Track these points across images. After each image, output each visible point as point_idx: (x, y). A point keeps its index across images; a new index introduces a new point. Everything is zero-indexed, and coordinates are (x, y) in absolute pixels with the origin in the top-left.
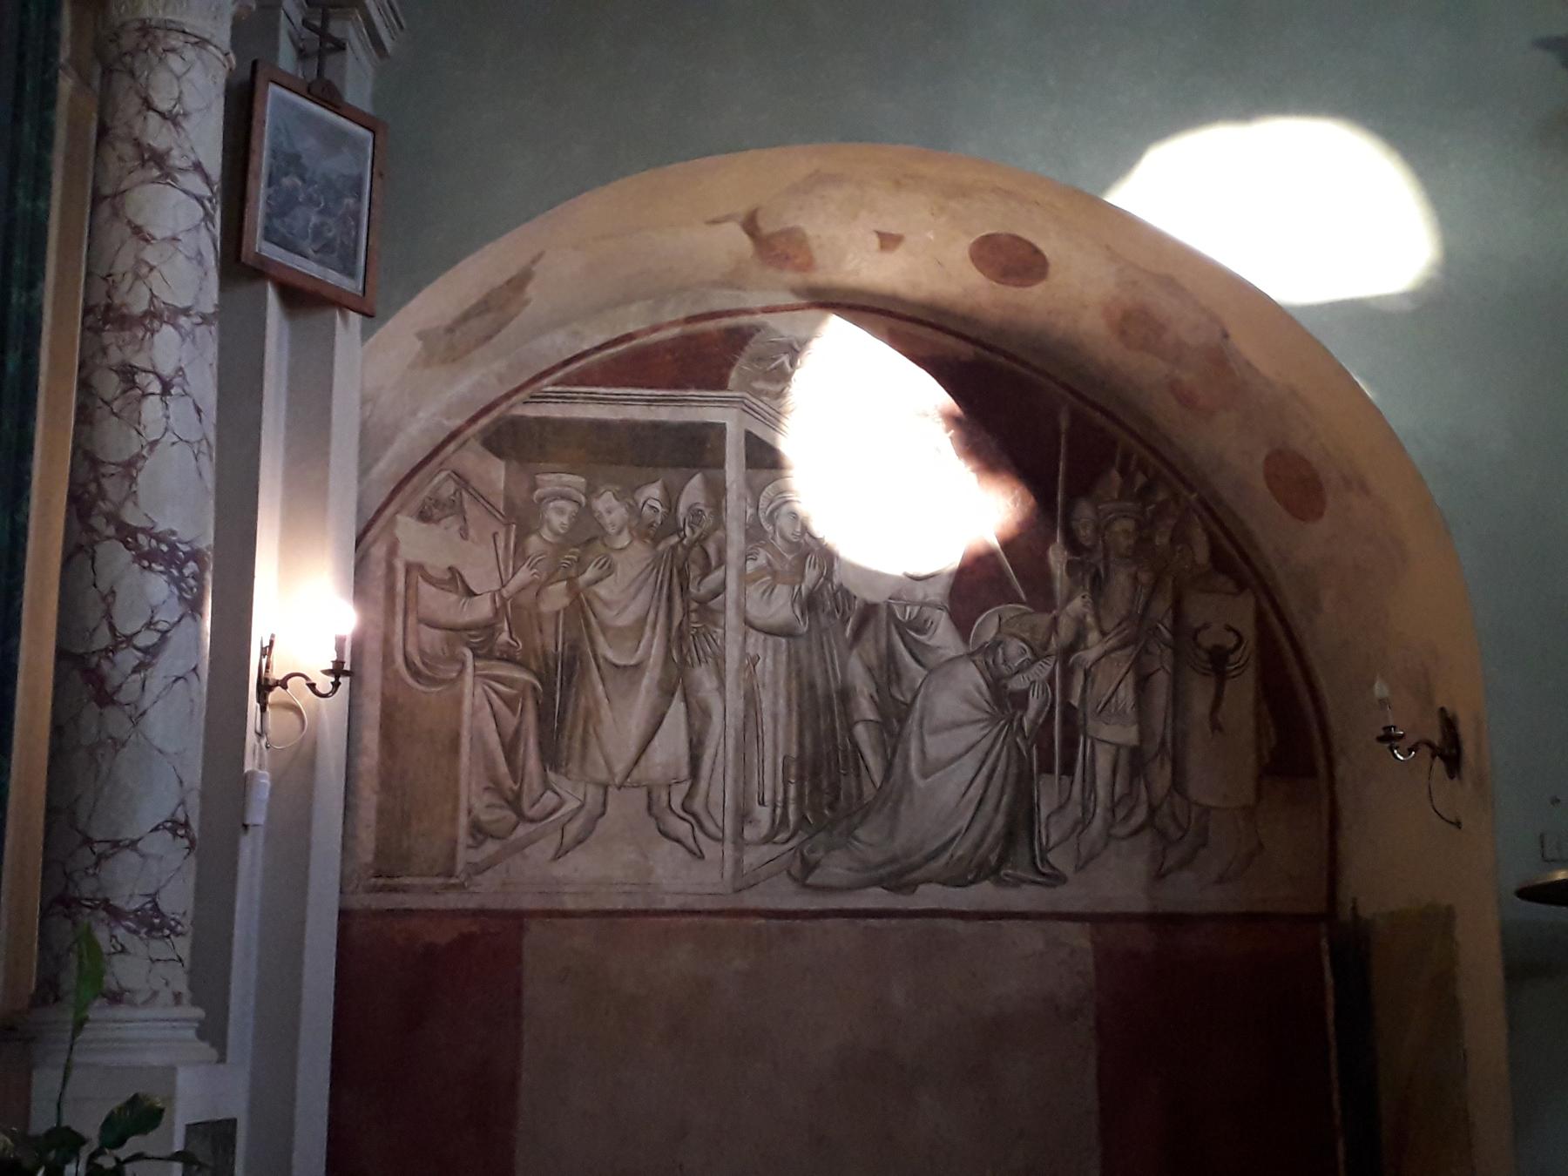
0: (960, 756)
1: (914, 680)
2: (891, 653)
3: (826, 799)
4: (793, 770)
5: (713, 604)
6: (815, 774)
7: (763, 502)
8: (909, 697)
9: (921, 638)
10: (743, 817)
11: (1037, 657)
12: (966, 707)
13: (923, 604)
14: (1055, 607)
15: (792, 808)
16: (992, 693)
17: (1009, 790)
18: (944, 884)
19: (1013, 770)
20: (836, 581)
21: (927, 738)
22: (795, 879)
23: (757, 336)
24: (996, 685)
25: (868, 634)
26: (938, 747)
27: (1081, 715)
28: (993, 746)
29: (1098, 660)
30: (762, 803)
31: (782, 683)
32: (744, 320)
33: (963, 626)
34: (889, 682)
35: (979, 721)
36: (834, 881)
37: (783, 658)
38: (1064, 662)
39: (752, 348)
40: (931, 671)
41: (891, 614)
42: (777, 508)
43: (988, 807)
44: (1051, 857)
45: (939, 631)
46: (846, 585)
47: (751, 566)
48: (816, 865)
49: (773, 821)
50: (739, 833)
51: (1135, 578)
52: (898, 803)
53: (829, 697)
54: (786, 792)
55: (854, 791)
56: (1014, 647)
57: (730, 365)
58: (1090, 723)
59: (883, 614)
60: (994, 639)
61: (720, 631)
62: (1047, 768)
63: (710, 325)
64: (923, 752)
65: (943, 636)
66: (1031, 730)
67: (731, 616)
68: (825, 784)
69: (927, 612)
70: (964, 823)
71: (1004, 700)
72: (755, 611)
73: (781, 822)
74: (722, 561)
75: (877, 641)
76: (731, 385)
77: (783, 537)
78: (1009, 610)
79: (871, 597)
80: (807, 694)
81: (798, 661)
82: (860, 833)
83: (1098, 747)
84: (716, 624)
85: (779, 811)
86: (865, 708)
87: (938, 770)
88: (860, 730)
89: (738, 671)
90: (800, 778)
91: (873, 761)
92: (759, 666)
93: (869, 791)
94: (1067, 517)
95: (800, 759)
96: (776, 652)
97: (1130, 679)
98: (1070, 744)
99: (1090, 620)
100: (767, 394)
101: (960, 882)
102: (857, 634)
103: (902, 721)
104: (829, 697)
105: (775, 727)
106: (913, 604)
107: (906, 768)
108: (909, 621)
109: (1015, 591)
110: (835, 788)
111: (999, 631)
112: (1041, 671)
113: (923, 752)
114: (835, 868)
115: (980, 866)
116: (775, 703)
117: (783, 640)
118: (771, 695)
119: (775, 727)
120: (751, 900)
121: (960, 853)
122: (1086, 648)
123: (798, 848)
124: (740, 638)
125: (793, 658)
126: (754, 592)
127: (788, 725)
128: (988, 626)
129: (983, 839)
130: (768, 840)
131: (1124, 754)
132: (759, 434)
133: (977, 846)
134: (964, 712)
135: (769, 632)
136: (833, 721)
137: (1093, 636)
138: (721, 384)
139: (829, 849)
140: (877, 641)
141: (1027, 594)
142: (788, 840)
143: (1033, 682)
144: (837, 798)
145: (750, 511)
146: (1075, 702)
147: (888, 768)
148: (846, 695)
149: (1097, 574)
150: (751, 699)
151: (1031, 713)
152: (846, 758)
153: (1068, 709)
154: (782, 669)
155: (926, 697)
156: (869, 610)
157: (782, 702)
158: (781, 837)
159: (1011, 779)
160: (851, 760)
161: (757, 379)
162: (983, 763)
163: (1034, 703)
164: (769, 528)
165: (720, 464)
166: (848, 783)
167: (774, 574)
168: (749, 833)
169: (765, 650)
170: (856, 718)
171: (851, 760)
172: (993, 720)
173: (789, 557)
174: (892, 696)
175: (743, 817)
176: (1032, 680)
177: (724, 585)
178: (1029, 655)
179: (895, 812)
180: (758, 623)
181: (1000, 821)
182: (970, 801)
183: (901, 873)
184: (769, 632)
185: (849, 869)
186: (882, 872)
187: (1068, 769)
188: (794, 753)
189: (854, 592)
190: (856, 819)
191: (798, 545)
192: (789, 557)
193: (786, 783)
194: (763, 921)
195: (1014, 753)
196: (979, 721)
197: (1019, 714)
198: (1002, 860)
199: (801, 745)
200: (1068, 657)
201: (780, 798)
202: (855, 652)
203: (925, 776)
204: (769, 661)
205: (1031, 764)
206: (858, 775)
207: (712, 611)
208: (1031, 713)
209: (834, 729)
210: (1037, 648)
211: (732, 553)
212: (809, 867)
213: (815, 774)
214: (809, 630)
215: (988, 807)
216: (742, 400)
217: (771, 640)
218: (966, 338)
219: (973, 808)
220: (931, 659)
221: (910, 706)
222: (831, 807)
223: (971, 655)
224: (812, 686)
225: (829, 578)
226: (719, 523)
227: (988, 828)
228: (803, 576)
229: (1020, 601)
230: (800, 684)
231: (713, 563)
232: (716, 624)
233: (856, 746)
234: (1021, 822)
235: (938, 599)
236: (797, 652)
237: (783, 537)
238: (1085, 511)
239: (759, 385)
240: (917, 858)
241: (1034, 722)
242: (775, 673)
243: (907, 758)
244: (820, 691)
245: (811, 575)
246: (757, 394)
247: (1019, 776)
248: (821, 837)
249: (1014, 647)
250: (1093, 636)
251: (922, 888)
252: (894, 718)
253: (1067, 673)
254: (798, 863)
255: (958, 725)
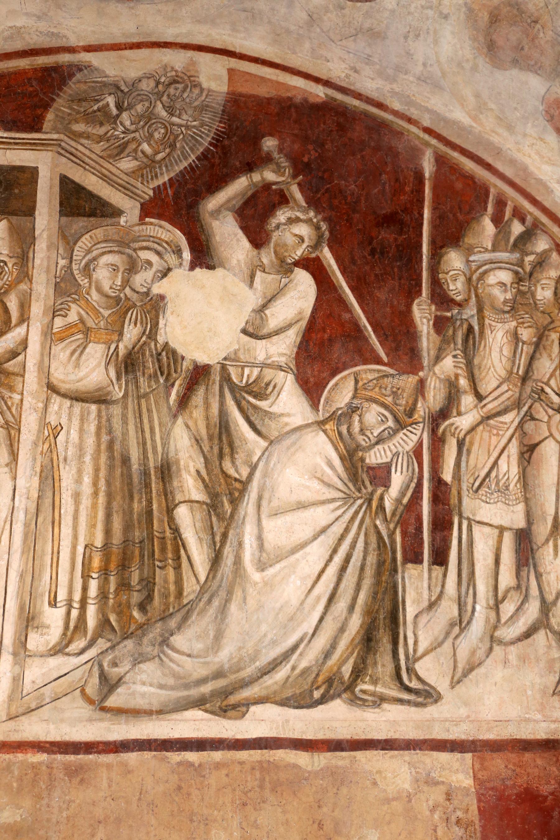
0: (303, 545)
1: (250, 455)
2: (223, 413)
3: (136, 598)
4: (96, 562)
5: (10, 366)
6: (124, 566)
7: (78, 253)
8: (245, 472)
9: (263, 404)
10: (29, 620)
11: (401, 425)
12: (316, 485)
13: (264, 365)
14: (422, 368)
15: (92, 611)
16: (346, 469)
17: (367, 583)
18: (284, 703)
19: (372, 559)
20: (161, 339)
21: (264, 522)
22: (91, 702)
23: (78, 76)
24: (352, 459)
25: (198, 398)
26: (279, 531)
27: (454, 492)
28: (347, 530)
29: (473, 429)
30: (53, 603)
31: (88, 459)
32: (65, 58)
33: (312, 390)
34: (221, 456)
35: (333, 500)
36: (141, 703)
37: (92, 428)
38: (434, 431)
39: (73, 87)
40: (271, 443)
41: (226, 378)
42: (95, 259)
43: (341, 605)
44: (420, 667)
45: (283, 395)
46: (172, 344)
47: (59, 322)
48: (119, 681)
49: (67, 627)
50: (22, 643)
51: (516, 337)
52: (228, 601)
53: (146, 473)
54: (85, 589)
55: (172, 587)
56: (373, 415)
57: (46, 106)
58: (466, 501)
59: (216, 377)
60: (349, 405)
61: (17, 397)
62: (417, 559)
63: (23, 63)
64: (260, 538)
65: (288, 402)
66: (394, 514)
67: (32, 380)
68: (135, 578)
69: (269, 374)
70: (309, 626)
71: (361, 474)
72: (63, 373)
73: (76, 628)
74: (24, 319)
75: (207, 405)
76: (47, 126)
77: (99, 290)
78: (368, 372)
79: (203, 359)
80: (118, 471)
81: (110, 432)
82: (178, 640)
83: (476, 529)
84: (11, 389)
85: (75, 613)
86: (189, 486)
87: (279, 559)
88: (183, 514)
89: (35, 444)
90: (105, 571)
91: (198, 552)
92: (61, 438)
93: (190, 587)
94: (434, 270)
95: (106, 546)
96: (82, 420)
97: (514, 449)
98: (442, 525)
99: (463, 382)
100: (88, 138)
101: (302, 701)
102: (184, 401)
103: (235, 502)
104: (146, 473)
105: (77, 511)
106: (253, 365)
107: (238, 561)
108: (247, 385)
109: (373, 351)
110: (148, 584)
111: (354, 397)
112: (406, 441)
113: (260, 538)
114: (143, 684)
115: (330, 681)
116: (79, 481)
117: (94, 407)
118: (74, 471)
119: (77, 511)
120: (34, 729)
121: (303, 664)
122: (459, 414)
123: (98, 661)
124: (41, 405)
125: (104, 427)
126: (62, 353)
127: (94, 506)
128: (341, 391)
129: (333, 646)
130: (58, 650)
131: (508, 540)
132: (77, 179)
133: (327, 655)
134: (315, 490)
135: (78, 398)
136: (150, 502)
137: (467, 400)
138: (35, 125)
139: (139, 659)
140: (207, 405)
141: (387, 355)
142: (83, 651)
143: (397, 454)
144: (150, 597)
145: (62, 262)
146: (447, 476)
147: (216, 560)
148: (166, 471)
149: (470, 329)
150: (49, 477)
151: (394, 491)
152: (163, 550)
153: (438, 484)
154: (90, 441)
155: (265, 475)
156: (200, 374)
157: (87, 480)
158: (75, 647)
159: (369, 572)
160: (169, 547)
161: (77, 122)
162: (335, 551)
163: (398, 479)
164: (84, 282)
165: (30, 212)
166: (165, 576)
167: (87, 331)
168: (35, 641)
169: (70, 419)
170: (179, 497)
171: (169, 547)
172: (348, 499)
173: (106, 313)
174: (223, 472)
175: (29, 620)
176: (397, 453)
177: (24, 343)
178: (391, 423)
179: (223, 610)
180: (64, 387)
181: (356, 622)
182: (318, 599)
183: (226, 693)
184: (78, 398)
185: (161, 687)
186: (206, 689)
187: (440, 558)
188: (99, 542)
189: (181, 351)
190: (172, 623)
191: (118, 300)
192: (106, 313)
193: (86, 577)
194: (42, 757)
195: (373, 539)
196: (333, 500)
197: (380, 491)
198: (358, 673)
199: (108, 532)
200: (438, 426)
201: (77, 596)
202: (180, 421)
203: (262, 567)
204: (74, 435)
205: (394, 552)
206: (178, 568)
207: (8, 374)
208: (394, 491)
209: (149, 513)
210: (400, 415)
211: (37, 309)
212: (109, 684)
213: (124, 566)
214: (126, 396)
215: (341, 605)
216: (58, 143)
217: (78, 407)
218: (317, 80)
219: (320, 608)
220: (273, 429)
221: (245, 484)
222: (142, 607)
223: (321, 424)
224: (126, 461)
225: (153, 335)
226: (25, 274)
227: (342, 630)
228: (121, 334)
229: (379, 362)
230: (111, 458)
231: (14, 321)
232: (11, 389)
233: (176, 531)
234: (383, 622)
235: (282, 360)
236: (109, 420)
237: (99, 290)
238: (454, 260)
239: (79, 127)
240: (248, 671)
241: (398, 501)
242: (81, 448)
243: (240, 544)
244: (135, 467)
245: (131, 333)
246: (76, 136)
247: (380, 564)
248: (129, 644)
249: (373, 415)
250: (467, 400)
251: (253, 709)
252: (225, 497)
253: (438, 442)
254: (95, 680)
255: (302, 506)
